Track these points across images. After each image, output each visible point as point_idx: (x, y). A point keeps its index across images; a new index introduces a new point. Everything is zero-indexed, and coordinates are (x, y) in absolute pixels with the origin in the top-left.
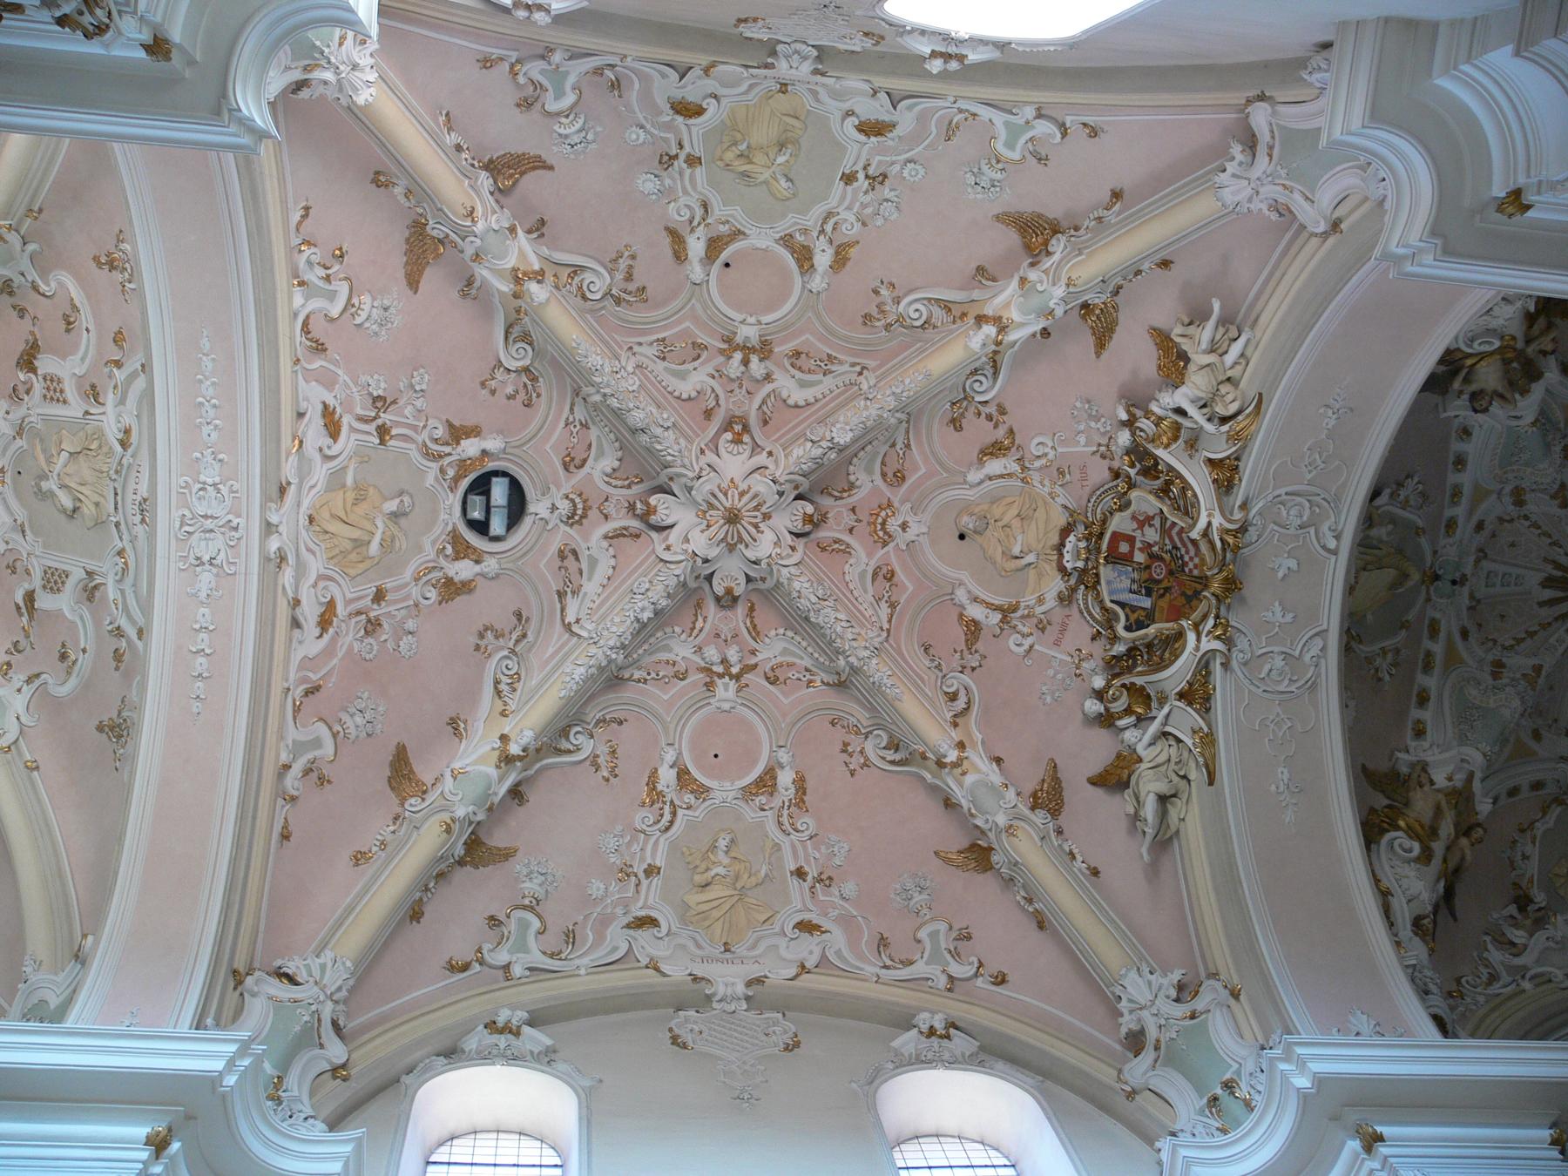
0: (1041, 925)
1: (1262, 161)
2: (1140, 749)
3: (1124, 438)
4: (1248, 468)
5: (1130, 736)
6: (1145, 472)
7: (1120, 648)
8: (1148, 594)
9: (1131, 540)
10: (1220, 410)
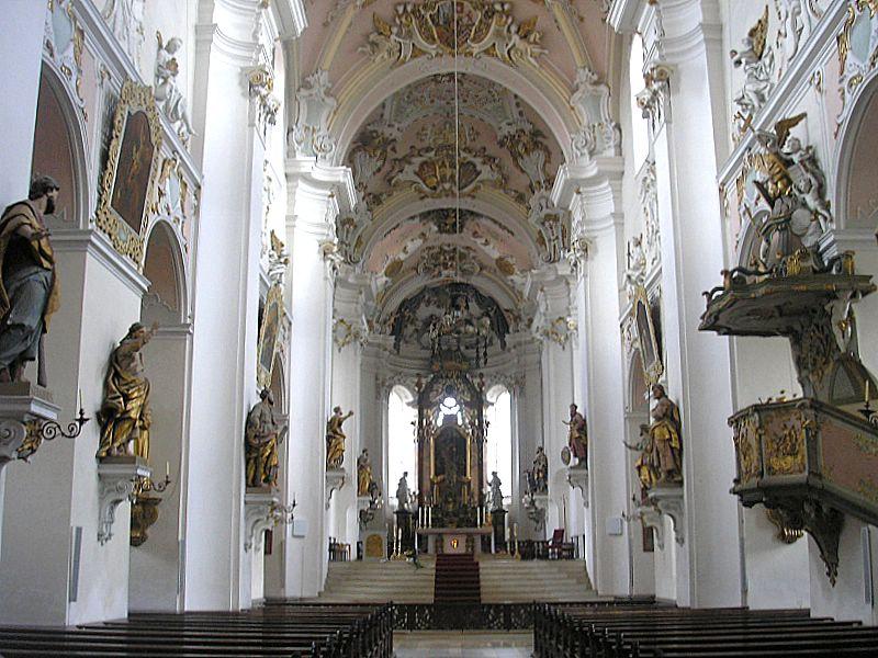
0: (325, 25)
1: (591, 88)
2: (393, 37)
3: (498, 7)
4: (493, 61)
5: (395, 30)
6: (486, 12)
7: (423, 12)
8: (445, 23)
9: (462, 11)
10: (512, 52)
